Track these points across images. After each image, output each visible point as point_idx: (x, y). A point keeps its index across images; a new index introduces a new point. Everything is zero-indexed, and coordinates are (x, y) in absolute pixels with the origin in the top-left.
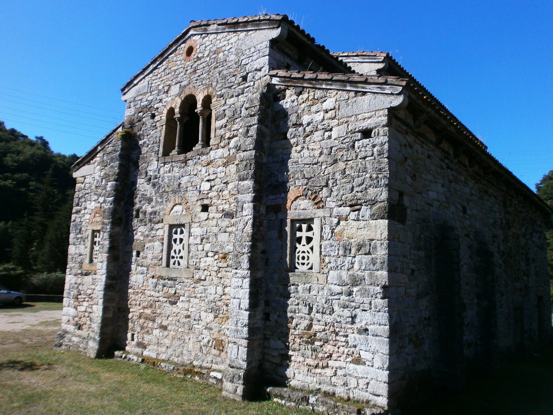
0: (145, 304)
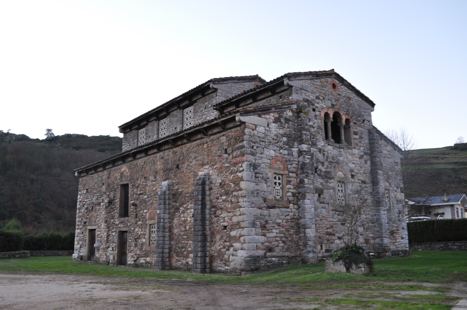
0: (328, 226)
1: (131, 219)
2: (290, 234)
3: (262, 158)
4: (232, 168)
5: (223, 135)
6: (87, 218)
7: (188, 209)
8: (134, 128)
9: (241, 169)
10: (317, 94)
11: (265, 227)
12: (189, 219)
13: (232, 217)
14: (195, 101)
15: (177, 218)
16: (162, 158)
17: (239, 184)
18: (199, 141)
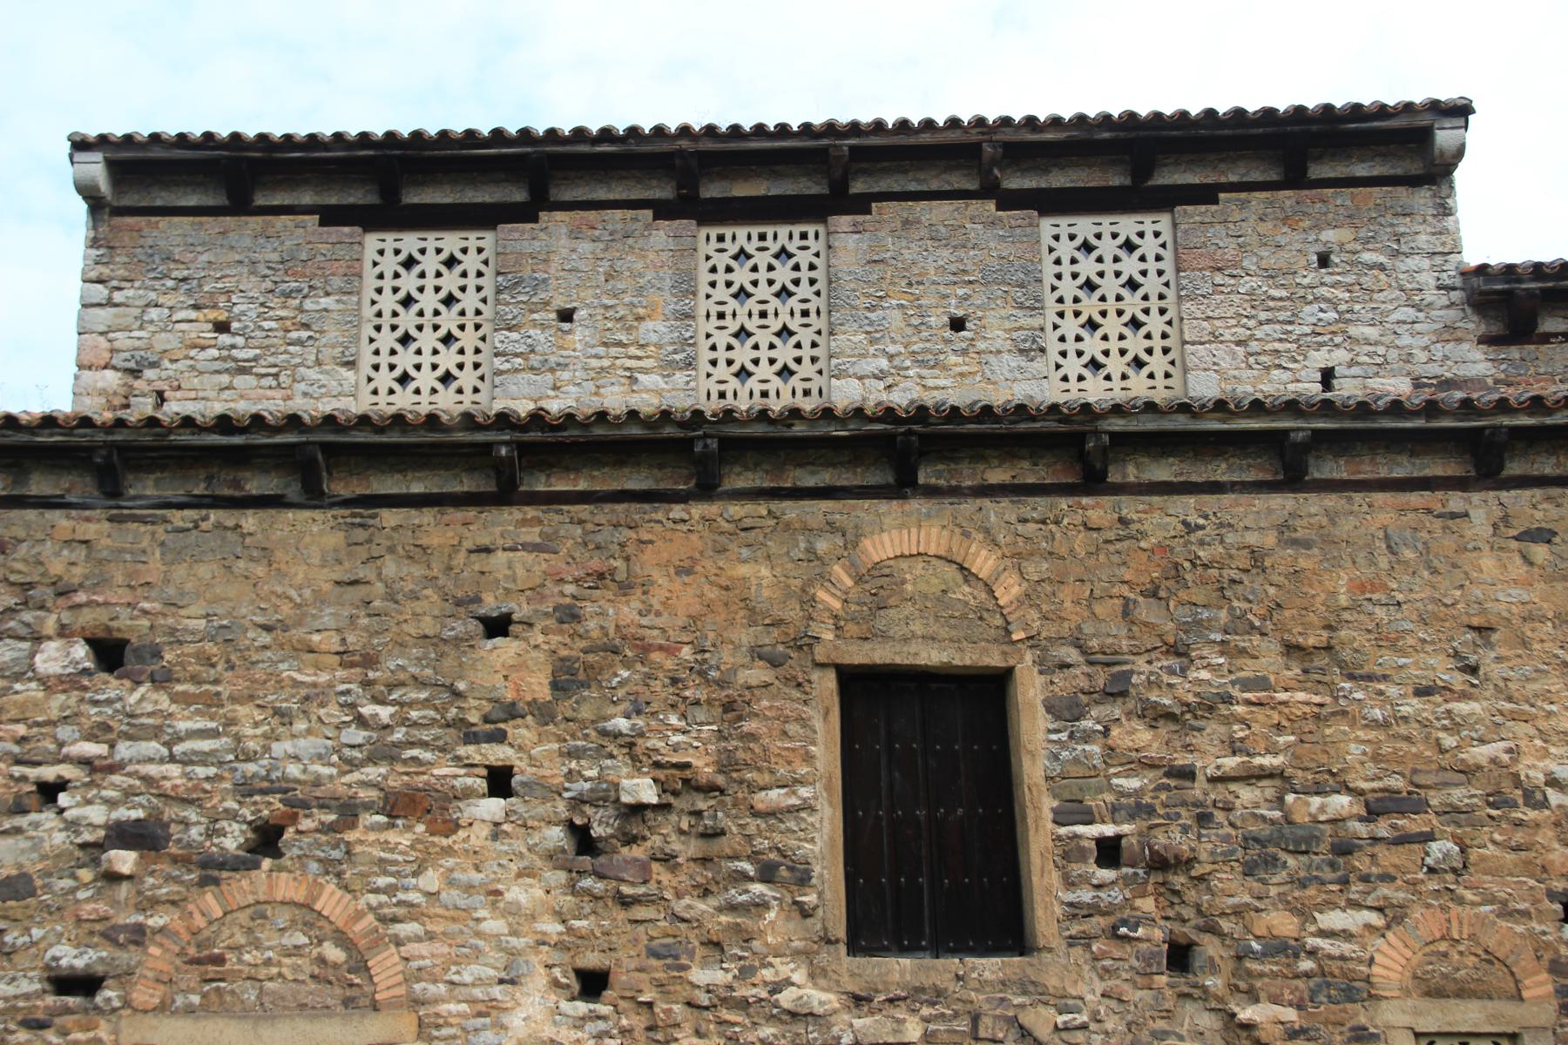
14: (1205, 195)
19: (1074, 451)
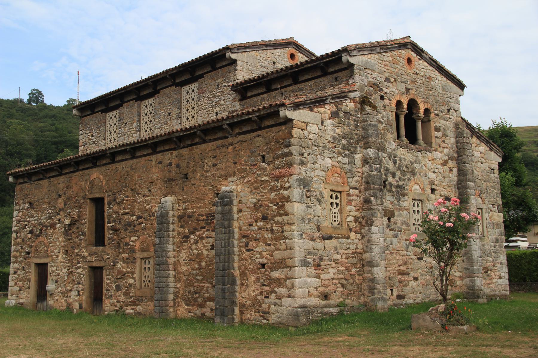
1: (109, 251)
2: (351, 275)
3: (314, 169)
4: (273, 184)
5: (258, 136)
6: (31, 247)
7: (202, 238)
8: (100, 109)
9: (287, 185)
10: (387, 75)
11: (319, 266)
12: (205, 252)
13: (273, 252)
14: (201, 76)
15: (186, 251)
16: (160, 163)
17: (284, 205)
18: (219, 142)
19: (111, 156)
